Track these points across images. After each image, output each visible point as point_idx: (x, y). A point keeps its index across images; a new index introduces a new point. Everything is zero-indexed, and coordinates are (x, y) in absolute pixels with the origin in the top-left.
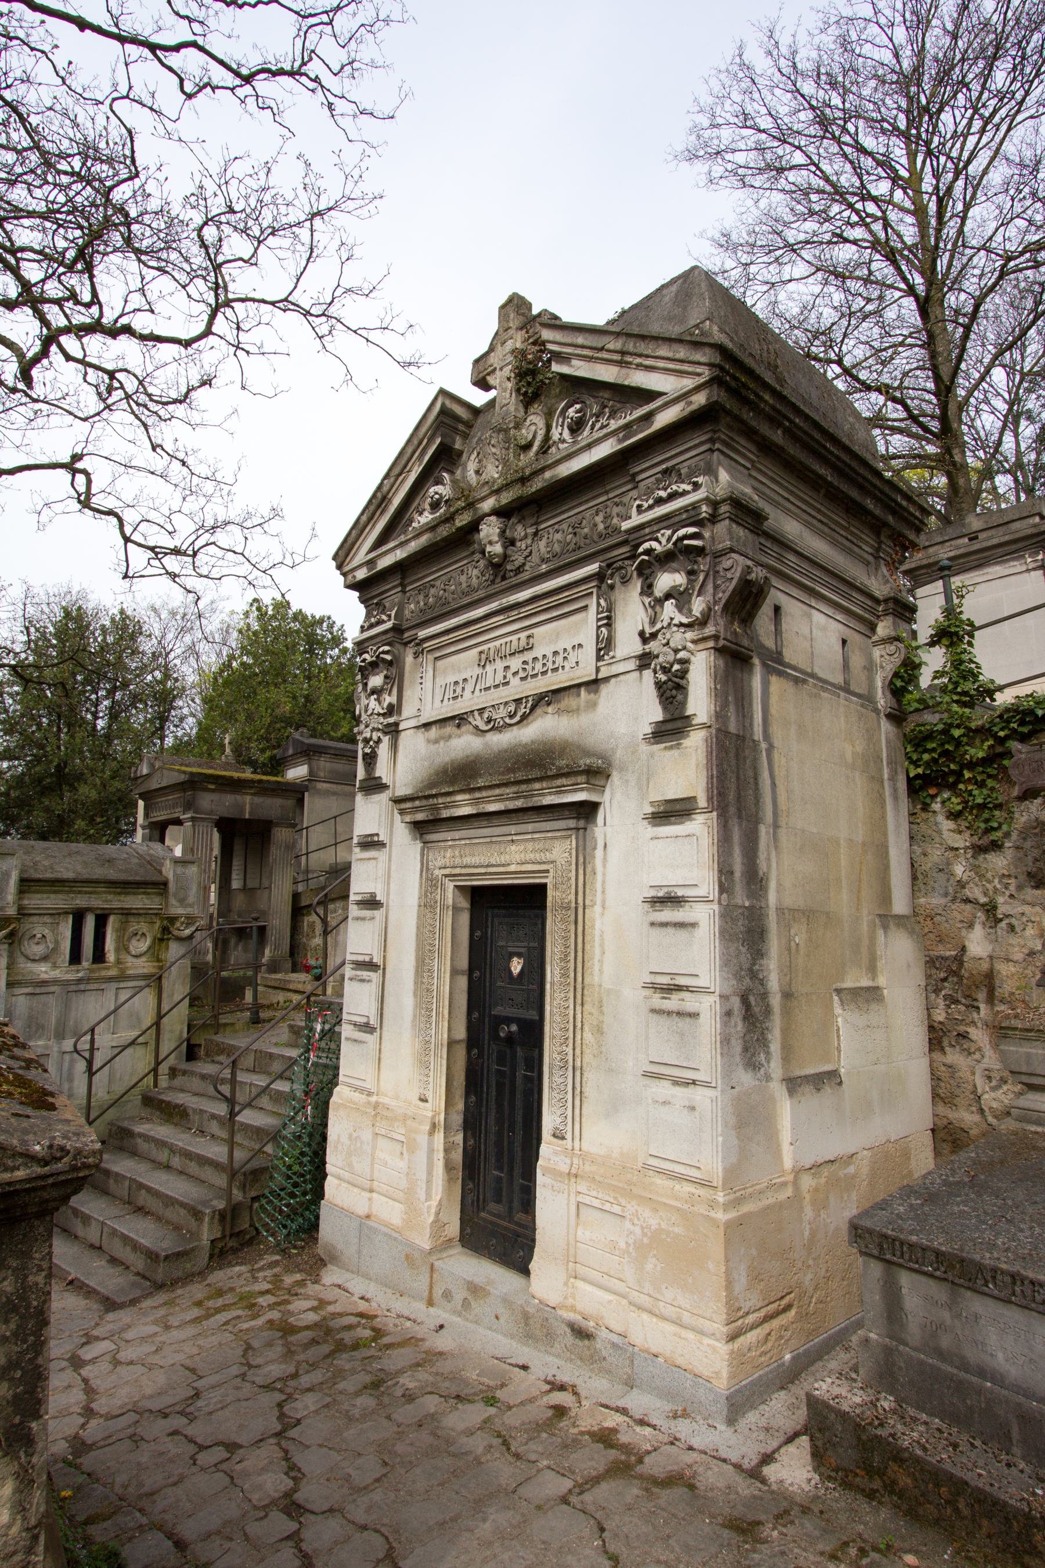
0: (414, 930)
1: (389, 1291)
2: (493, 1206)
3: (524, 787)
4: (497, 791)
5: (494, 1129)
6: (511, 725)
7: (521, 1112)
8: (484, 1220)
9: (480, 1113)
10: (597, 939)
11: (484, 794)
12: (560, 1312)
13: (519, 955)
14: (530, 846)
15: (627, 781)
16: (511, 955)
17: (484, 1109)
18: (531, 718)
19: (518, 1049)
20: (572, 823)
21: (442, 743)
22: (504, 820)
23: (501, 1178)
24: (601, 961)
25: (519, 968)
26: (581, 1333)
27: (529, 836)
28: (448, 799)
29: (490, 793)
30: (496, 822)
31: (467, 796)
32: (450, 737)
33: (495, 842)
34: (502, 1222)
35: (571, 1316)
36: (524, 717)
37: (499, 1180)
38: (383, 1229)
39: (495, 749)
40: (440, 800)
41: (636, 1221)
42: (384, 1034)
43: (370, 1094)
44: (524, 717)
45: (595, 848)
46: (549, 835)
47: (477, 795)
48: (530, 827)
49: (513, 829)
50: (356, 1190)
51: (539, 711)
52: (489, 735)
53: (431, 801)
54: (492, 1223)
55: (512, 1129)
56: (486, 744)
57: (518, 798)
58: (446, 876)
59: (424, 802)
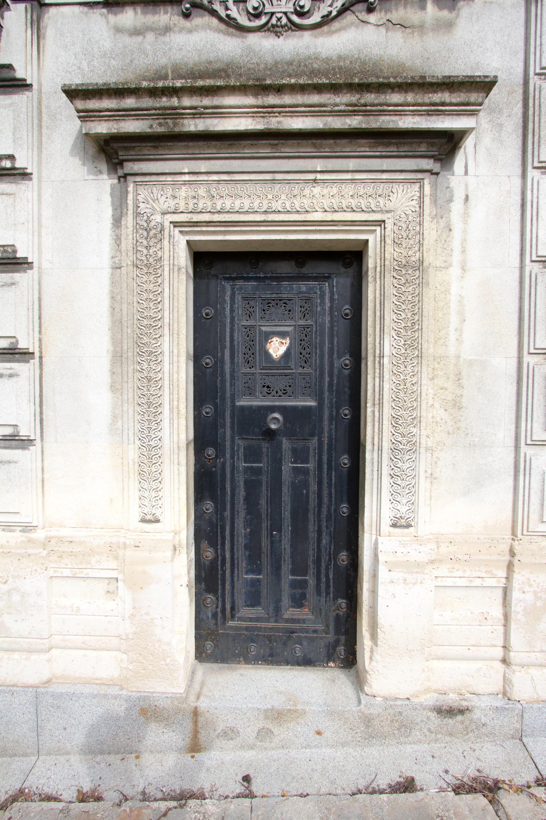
0: (106, 302)
1: (111, 758)
2: (245, 612)
3: (370, 98)
4: (315, 99)
5: (241, 530)
6: (300, 28)
7: (289, 508)
8: (236, 628)
9: (223, 519)
10: (454, 306)
11: (287, 99)
12: (416, 700)
13: (282, 335)
14: (349, 189)
15: (501, 125)
16: (268, 336)
17: (228, 513)
18: (336, 25)
19: (284, 440)
20: (427, 164)
21: (150, 37)
22: (306, 149)
23: (259, 580)
24: (459, 330)
25: (282, 350)
26: (449, 712)
27: (349, 176)
28: (207, 101)
29: (299, 99)
30: (288, 151)
31: (250, 100)
32: (167, 29)
33: (280, 181)
34: (263, 625)
35: (430, 699)
36: (327, 20)
37: (255, 583)
38: (87, 690)
39: (269, 59)
40: (187, 102)
41: (527, 589)
42: (46, 446)
43: (27, 528)
44: (327, 20)
45: (450, 200)
46: (385, 176)
47: (272, 100)
48: (352, 164)
49: (319, 165)
50: (16, 656)
51: (349, 17)
52: (253, 39)
53: (164, 101)
54: (247, 629)
55: (276, 525)
56: (250, 49)
57: (354, 113)
58: (176, 224)
59: (147, 102)
